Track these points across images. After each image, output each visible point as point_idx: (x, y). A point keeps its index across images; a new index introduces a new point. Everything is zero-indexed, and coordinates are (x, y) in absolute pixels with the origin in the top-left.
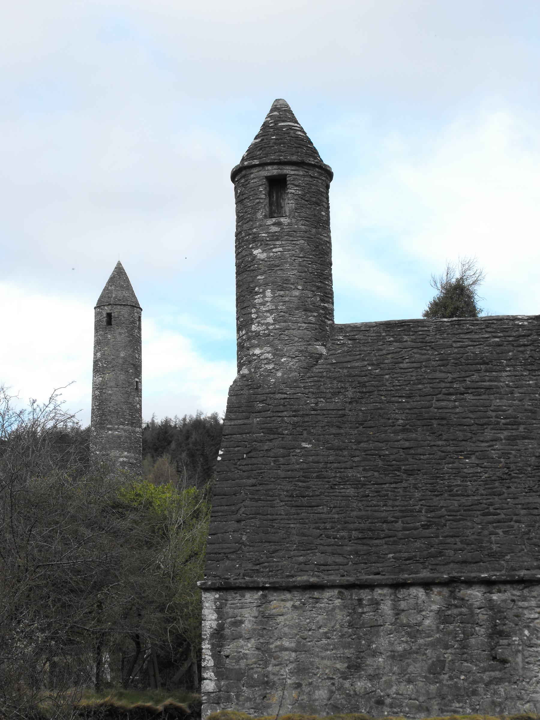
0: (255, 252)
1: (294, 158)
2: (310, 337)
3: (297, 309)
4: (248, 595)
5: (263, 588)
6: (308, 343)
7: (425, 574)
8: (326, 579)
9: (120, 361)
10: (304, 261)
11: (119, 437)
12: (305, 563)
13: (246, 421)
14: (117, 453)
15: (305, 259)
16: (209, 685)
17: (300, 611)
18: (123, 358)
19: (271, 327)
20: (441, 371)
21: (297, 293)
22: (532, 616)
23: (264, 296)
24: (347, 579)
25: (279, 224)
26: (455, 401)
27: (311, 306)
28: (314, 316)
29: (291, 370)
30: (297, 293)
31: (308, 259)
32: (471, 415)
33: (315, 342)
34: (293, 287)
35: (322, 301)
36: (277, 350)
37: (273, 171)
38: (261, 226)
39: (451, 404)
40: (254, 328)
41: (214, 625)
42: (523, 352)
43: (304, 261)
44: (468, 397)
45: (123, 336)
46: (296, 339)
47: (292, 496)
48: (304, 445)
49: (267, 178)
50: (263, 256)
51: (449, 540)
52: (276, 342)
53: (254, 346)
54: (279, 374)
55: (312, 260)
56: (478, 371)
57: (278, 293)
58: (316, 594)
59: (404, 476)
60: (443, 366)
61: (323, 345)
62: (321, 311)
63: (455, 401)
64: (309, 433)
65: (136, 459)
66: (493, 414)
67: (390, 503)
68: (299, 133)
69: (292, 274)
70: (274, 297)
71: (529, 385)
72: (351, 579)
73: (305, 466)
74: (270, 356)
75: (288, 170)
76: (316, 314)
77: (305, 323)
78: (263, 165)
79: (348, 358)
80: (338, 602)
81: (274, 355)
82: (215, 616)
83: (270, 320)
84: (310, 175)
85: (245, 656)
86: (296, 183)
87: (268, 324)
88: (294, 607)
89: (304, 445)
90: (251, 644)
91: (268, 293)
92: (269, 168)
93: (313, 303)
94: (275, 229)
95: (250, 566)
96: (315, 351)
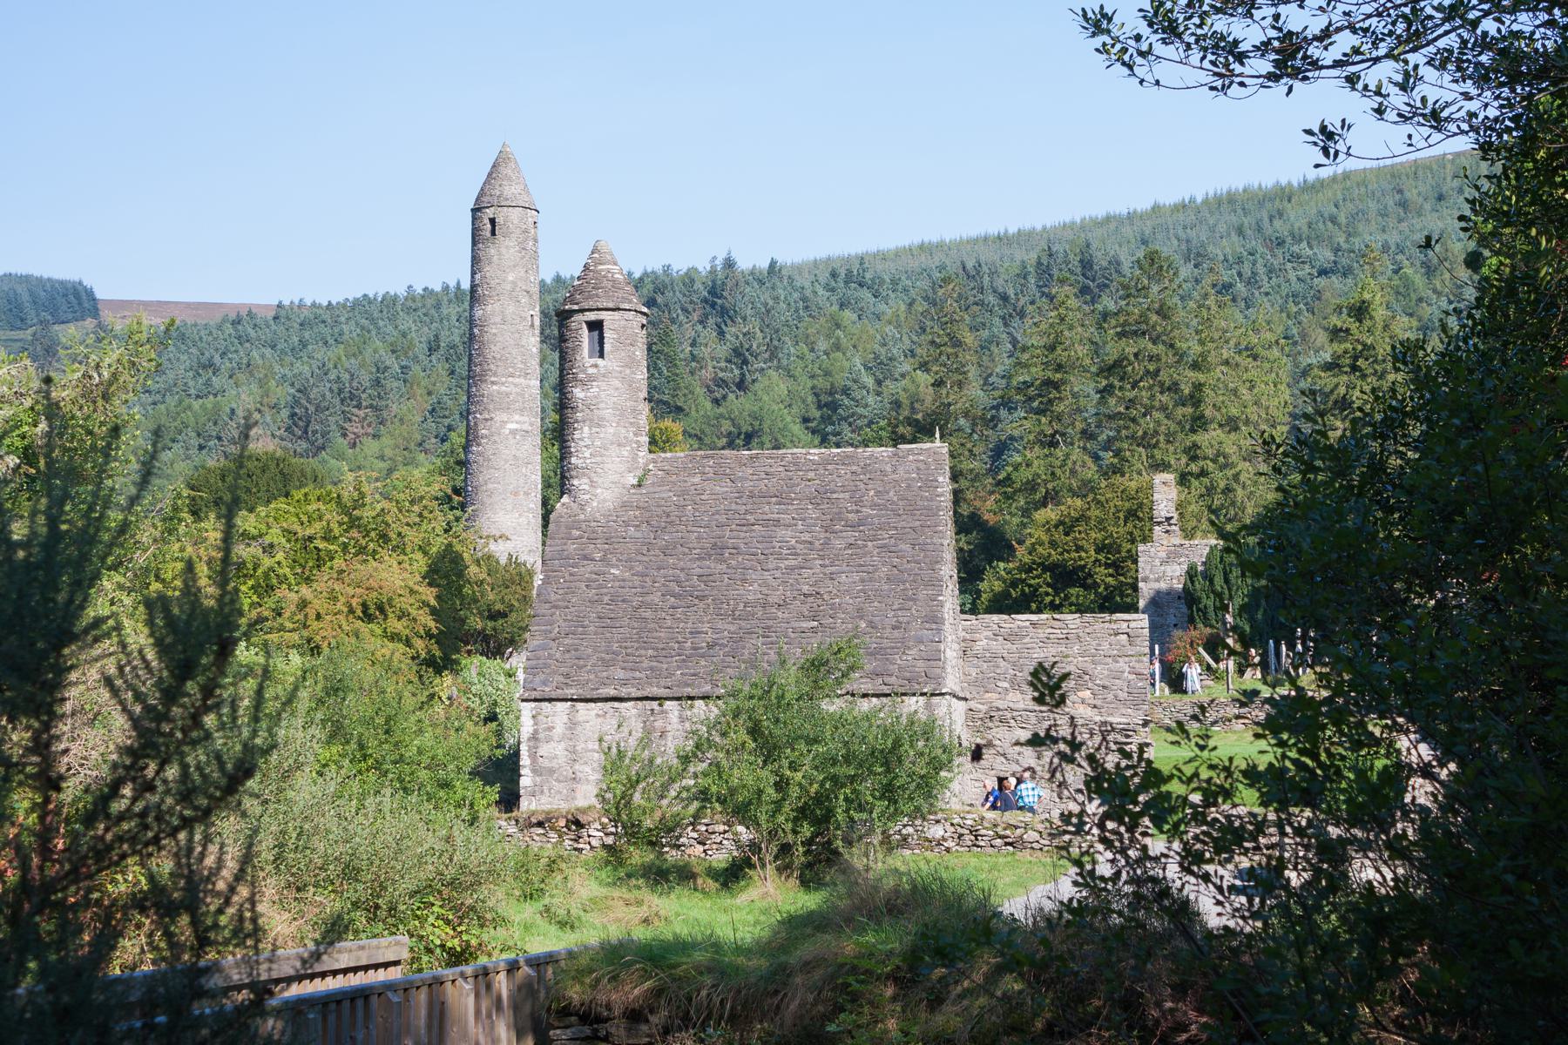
1: (611, 305)
3: (612, 444)
4: (559, 704)
5: (572, 700)
7: (707, 688)
8: (624, 692)
9: (509, 287)
11: (508, 394)
14: (505, 417)
16: (526, 781)
17: (600, 720)
18: (514, 283)
24: (639, 694)
25: (596, 366)
29: (605, 501)
32: (758, 545)
37: (592, 316)
39: (743, 535)
41: (531, 730)
45: (512, 250)
48: (612, 571)
51: (727, 659)
54: (595, 504)
57: (594, 430)
58: (616, 704)
59: (696, 602)
65: (531, 425)
67: (682, 625)
68: (617, 276)
72: (645, 693)
73: (612, 590)
74: (586, 487)
80: (634, 711)
82: (532, 722)
83: (587, 454)
85: (556, 757)
88: (598, 715)
90: (562, 745)
94: (591, 371)
95: (561, 679)
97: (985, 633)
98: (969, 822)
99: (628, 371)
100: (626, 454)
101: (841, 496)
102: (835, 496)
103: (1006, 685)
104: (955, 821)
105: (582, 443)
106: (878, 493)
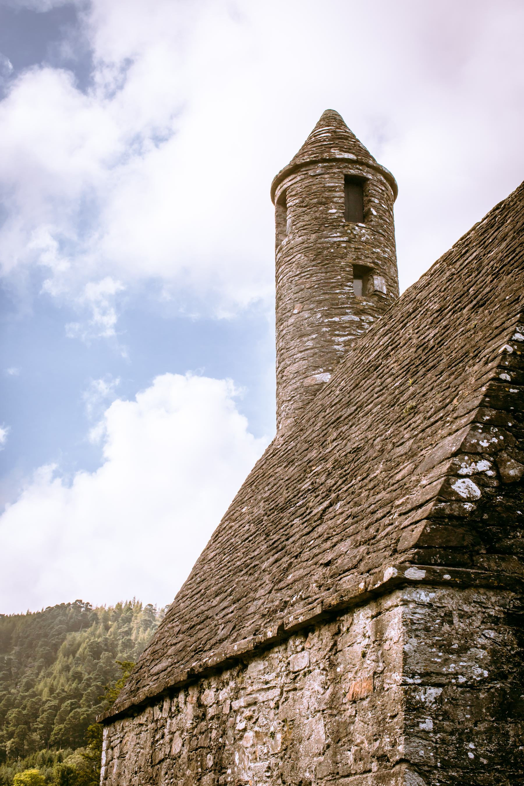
2: (305, 367)
3: (292, 339)
6: (304, 376)
10: (301, 277)
15: (303, 275)
22: (241, 726)
27: (308, 328)
28: (313, 339)
30: (291, 320)
31: (306, 274)
33: (314, 370)
34: (289, 314)
35: (327, 316)
43: (301, 277)
46: (291, 376)
55: (311, 272)
61: (325, 371)
62: (324, 329)
76: (314, 336)
77: (301, 352)
84: (311, 175)
86: (294, 193)
93: (311, 324)
96: (313, 383)
99: (314, 236)
100: (310, 344)
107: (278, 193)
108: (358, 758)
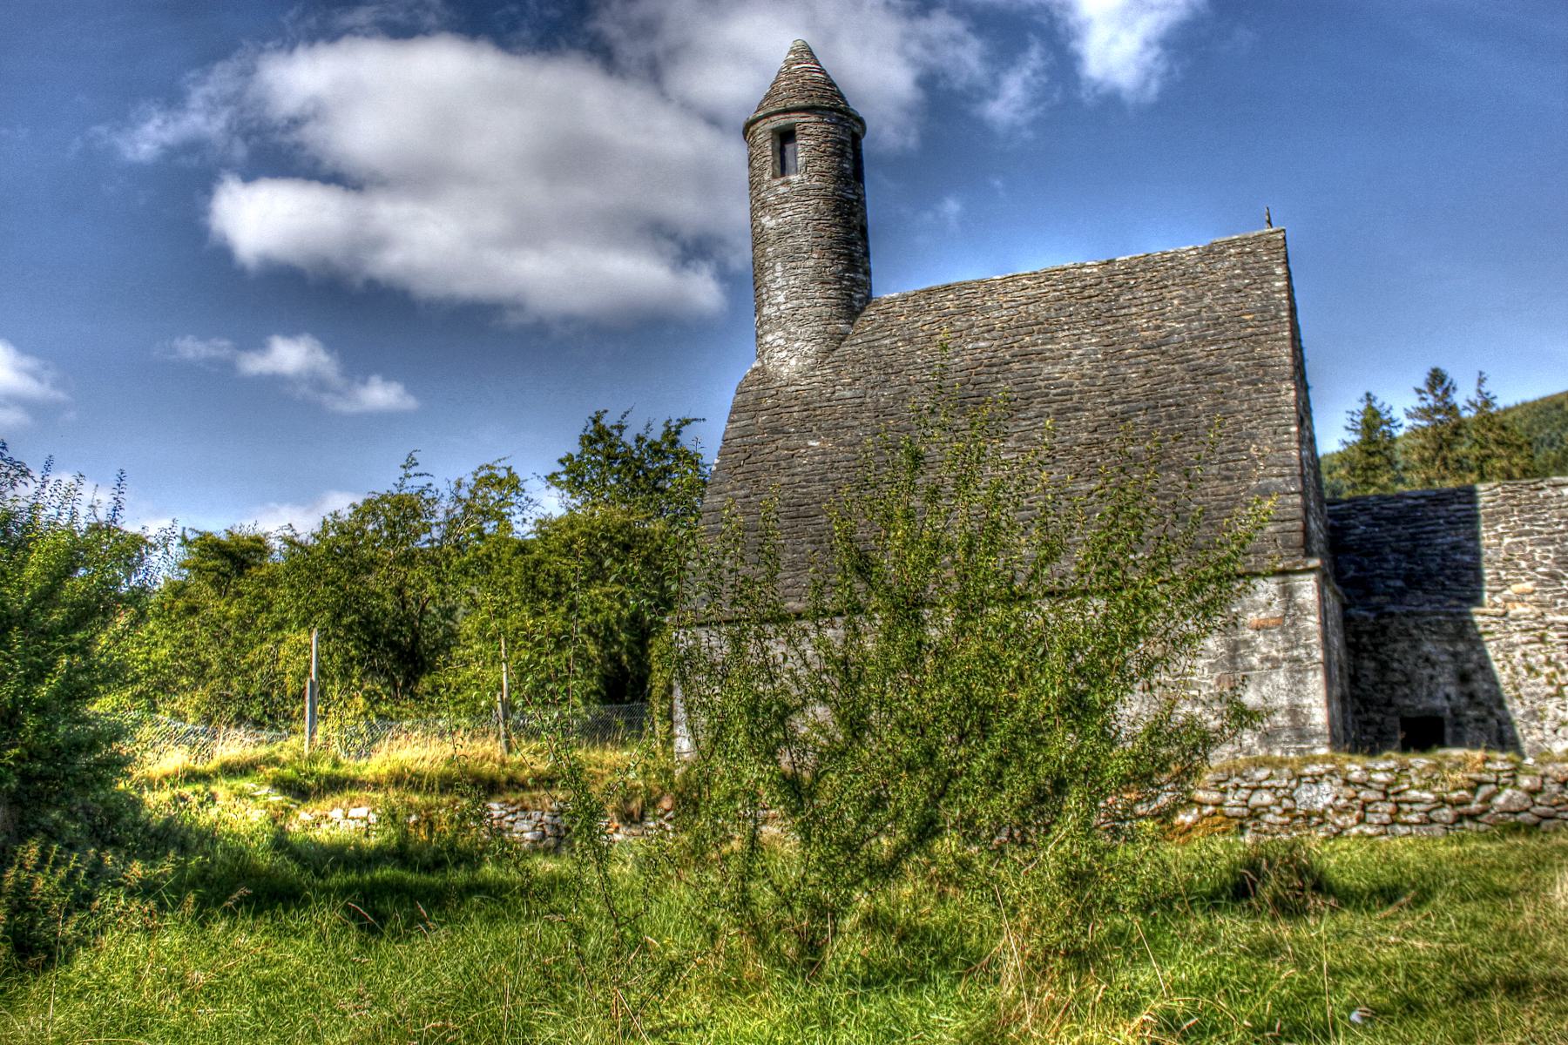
0: (764, 220)
3: (812, 282)
12: (793, 586)
13: (749, 422)
19: (782, 307)
20: (985, 340)
21: (811, 263)
23: (775, 271)
25: (788, 183)
26: (997, 373)
36: (789, 333)
38: (768, 188)
40: (766, 311)
42: (1087, 305)
44: (1015, 366)
47: (788, 505)
48: (811, 443)
49: (774, 131)
50: (773, 223)
52: (789, 324)
53: (766, 333)
56: (1030, 334)
60: (989, 331)
63: (997, 373)
64: (819, 429)
66: (1042, 384)
69: (803, 241)
70: (784, 272)
71: (1091, 344)
74: (782, 342)
75: (795, 118)
78: (767, 116)
79: (878, 335)
81: (787, 339)
83: (781, 299)
86: (806, 132)
87: (778, 304)
89: (811, 443)
91: (779, 267)
92: (775, 118)
94: (782, 190)
97: (1362, 518)
98: (1381, 777)
101: (1134, 310)
102: (1123, 311)
103: (1399, 583)
104: (1355, 776)
105: (774, 286)
106: (1185, 300)
107: (780, 121)
108: (1265, 659)
